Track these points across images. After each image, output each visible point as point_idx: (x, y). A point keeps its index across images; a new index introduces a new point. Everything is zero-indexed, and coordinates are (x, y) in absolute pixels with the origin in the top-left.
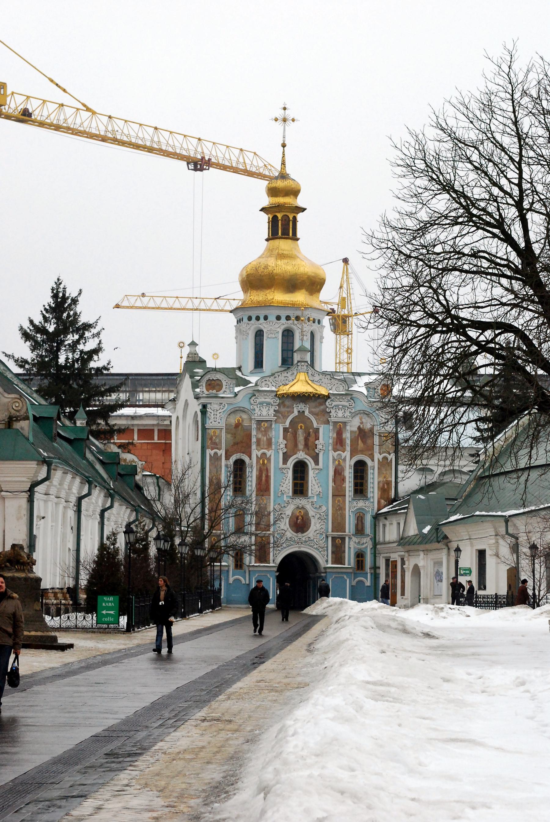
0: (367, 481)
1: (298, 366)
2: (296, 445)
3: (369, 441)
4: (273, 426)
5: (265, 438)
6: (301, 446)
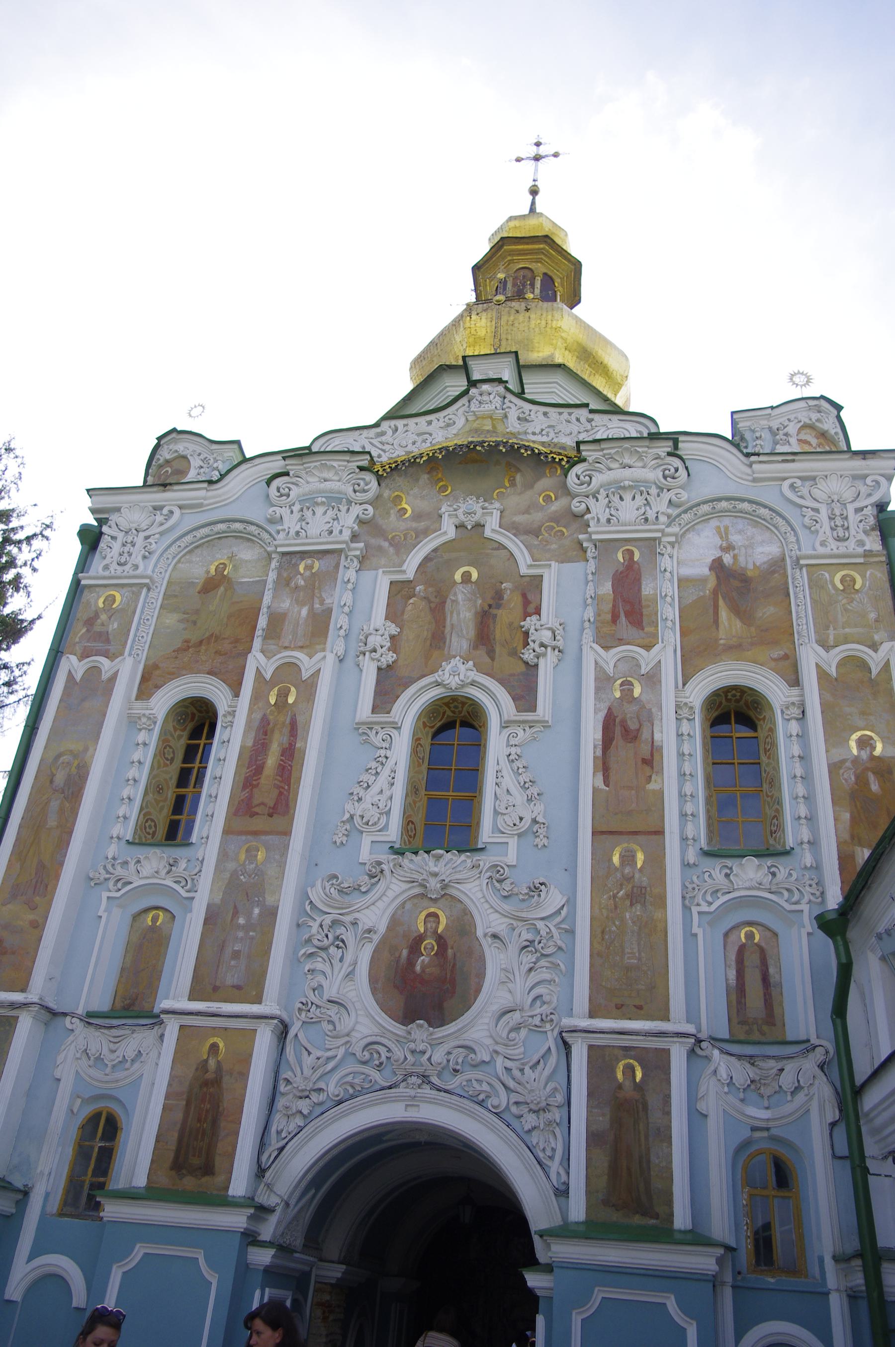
0: (774, 782)
2: (437, 640)
3: (767, 612)
5: (304, 612)
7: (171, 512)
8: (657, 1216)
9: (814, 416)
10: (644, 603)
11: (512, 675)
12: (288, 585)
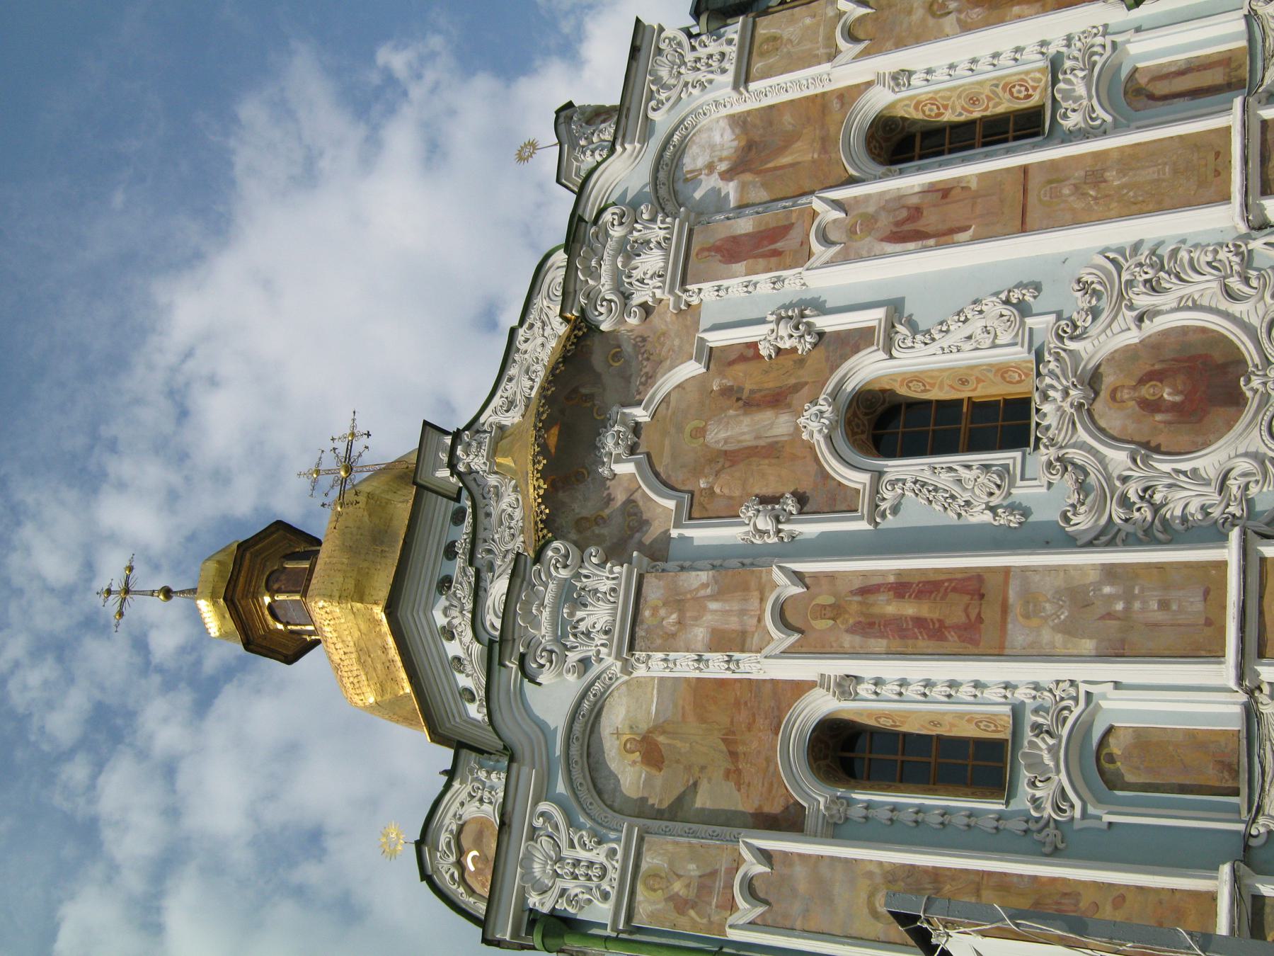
2: (772, 451)
5: (713, 606)
6: (777, 425)
7: (542, 814)
10: (763, 228)
11: (827, 359)
12: (674, 635)
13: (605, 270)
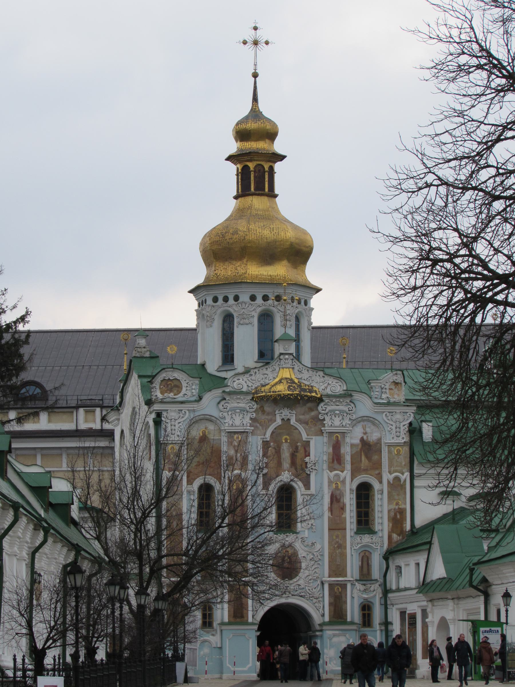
0: (373, 510)
1: (280, 359)
2: (279, 464)
3: (375, 457)
4: (250, 439)
6: (286, 464)
8: (344, 619)
9: (395, 378)
12: (232, 444)
13: (334, 407)
